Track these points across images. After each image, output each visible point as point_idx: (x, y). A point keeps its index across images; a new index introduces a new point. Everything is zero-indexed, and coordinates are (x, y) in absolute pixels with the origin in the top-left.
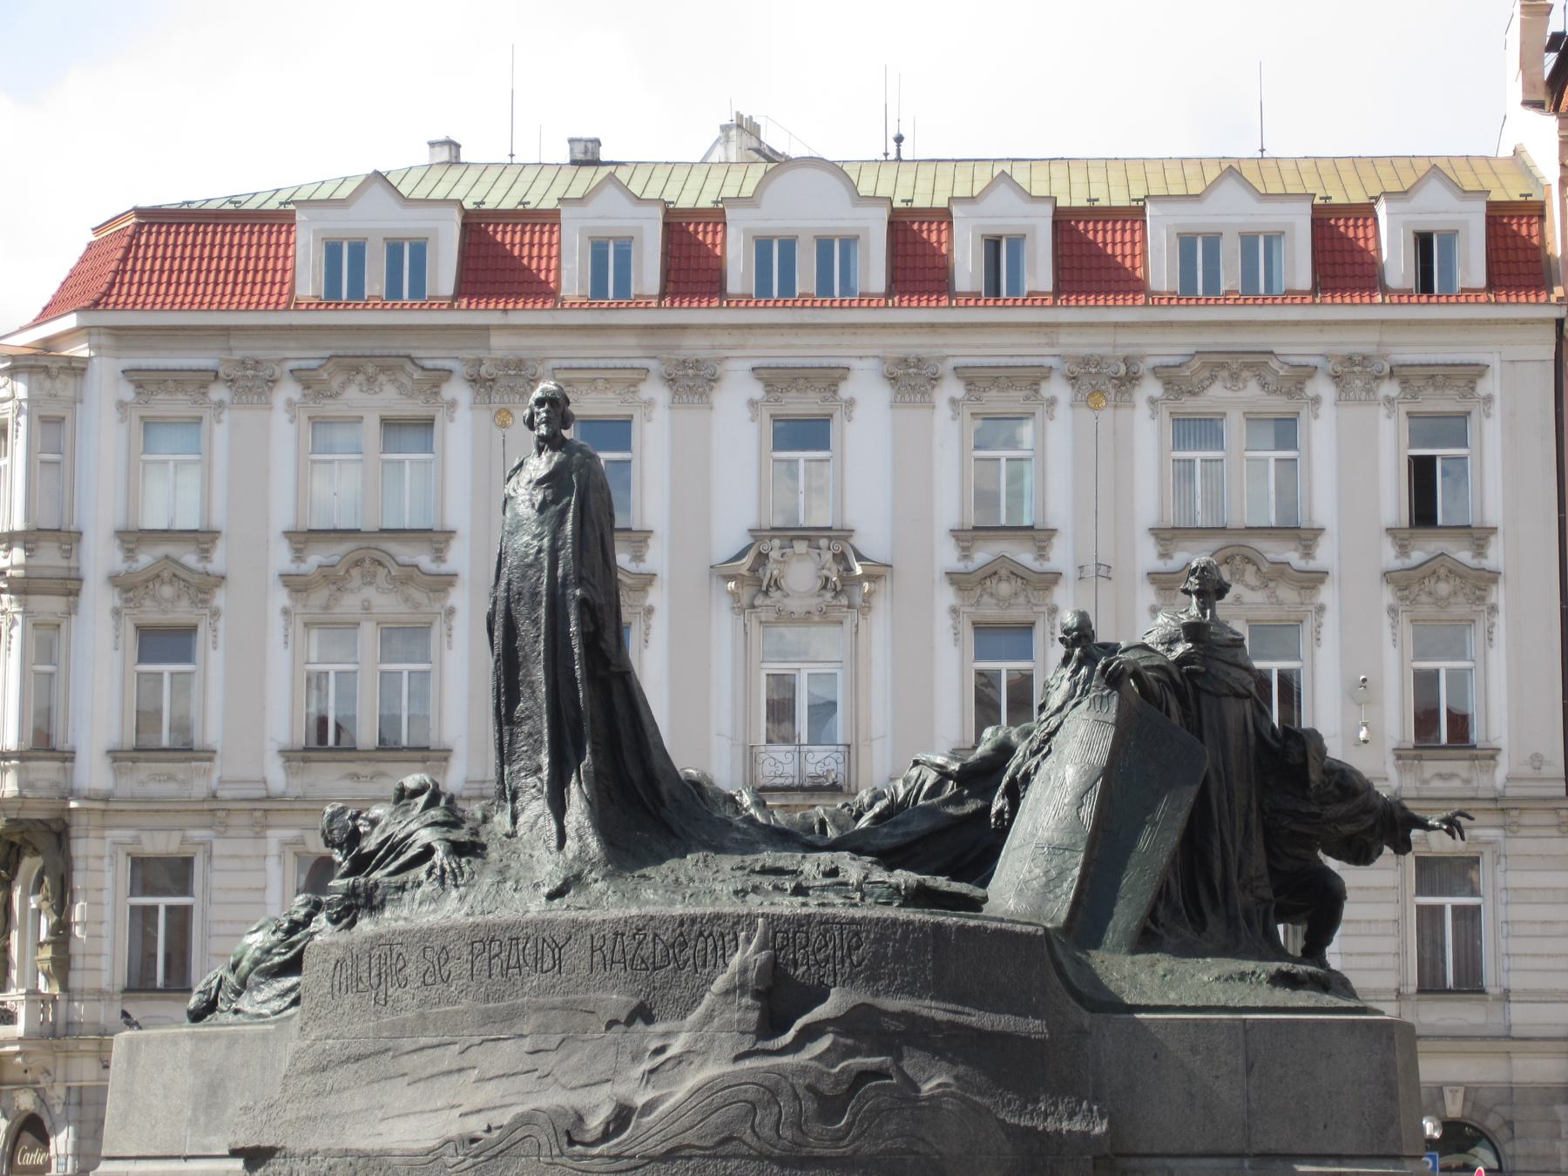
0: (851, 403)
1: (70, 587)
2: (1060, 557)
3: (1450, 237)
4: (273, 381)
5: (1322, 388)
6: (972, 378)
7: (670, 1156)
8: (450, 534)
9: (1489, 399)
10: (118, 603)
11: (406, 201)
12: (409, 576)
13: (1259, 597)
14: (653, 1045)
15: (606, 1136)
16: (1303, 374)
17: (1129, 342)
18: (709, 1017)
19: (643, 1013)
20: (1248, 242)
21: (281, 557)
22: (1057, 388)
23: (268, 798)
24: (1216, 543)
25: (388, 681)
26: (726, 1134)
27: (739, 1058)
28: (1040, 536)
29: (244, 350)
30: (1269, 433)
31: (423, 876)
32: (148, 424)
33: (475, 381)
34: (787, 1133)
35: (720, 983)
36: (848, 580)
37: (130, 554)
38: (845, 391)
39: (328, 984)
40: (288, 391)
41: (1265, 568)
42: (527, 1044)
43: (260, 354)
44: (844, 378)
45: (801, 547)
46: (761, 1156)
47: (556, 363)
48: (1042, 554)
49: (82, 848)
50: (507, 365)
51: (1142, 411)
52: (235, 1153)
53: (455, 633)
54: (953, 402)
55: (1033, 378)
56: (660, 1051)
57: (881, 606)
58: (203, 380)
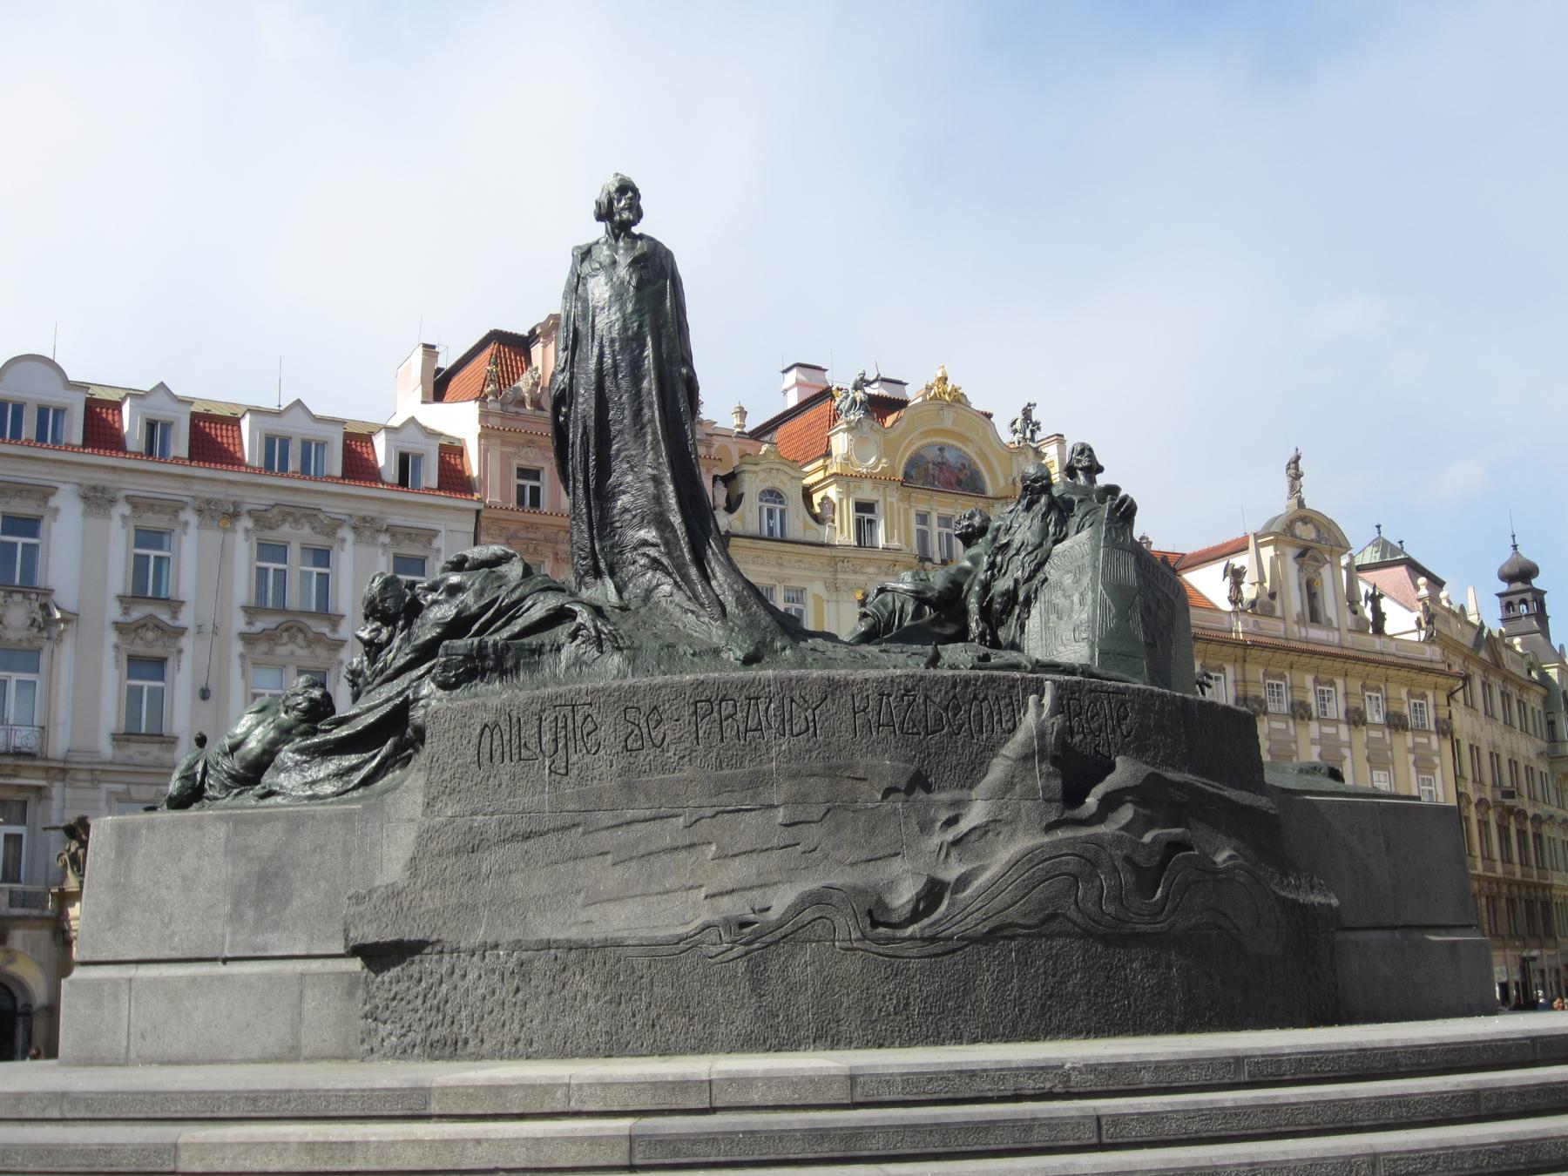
0: (56, 510)
2: (186, 618)
3: (419, 458)
5: (346, 533)
6: (135, 503)
7: (992, 936)
9: (438, 550)
13: (305, 652)
14: (944, 815)
15: (915, 916)
16: (337, 524)
17: (236, 493)
18: (1008, 785)
19: (919, 782)
20: (306, 445)
22: (189, 516)
24: (280, 619)
26: (1050, 910)
27: (1050, 828)
28: (175, 605)
30: (310, 556)
31: (563, 639)
34: (1109, 908)
35: (1013, 747)
36: (49, 620)
38: (53, 502)
39: (472, 751)
41: (310, 635)
42: (781, 815)
44: (53, 494)
45: (18, 597)
46: (1086, 934)
48: (175, 615)
51: (240, 535)
52: (357, 951)
54: (123, 517)
55: (175, 508)
56: (952, 822)
57: (69, 640)
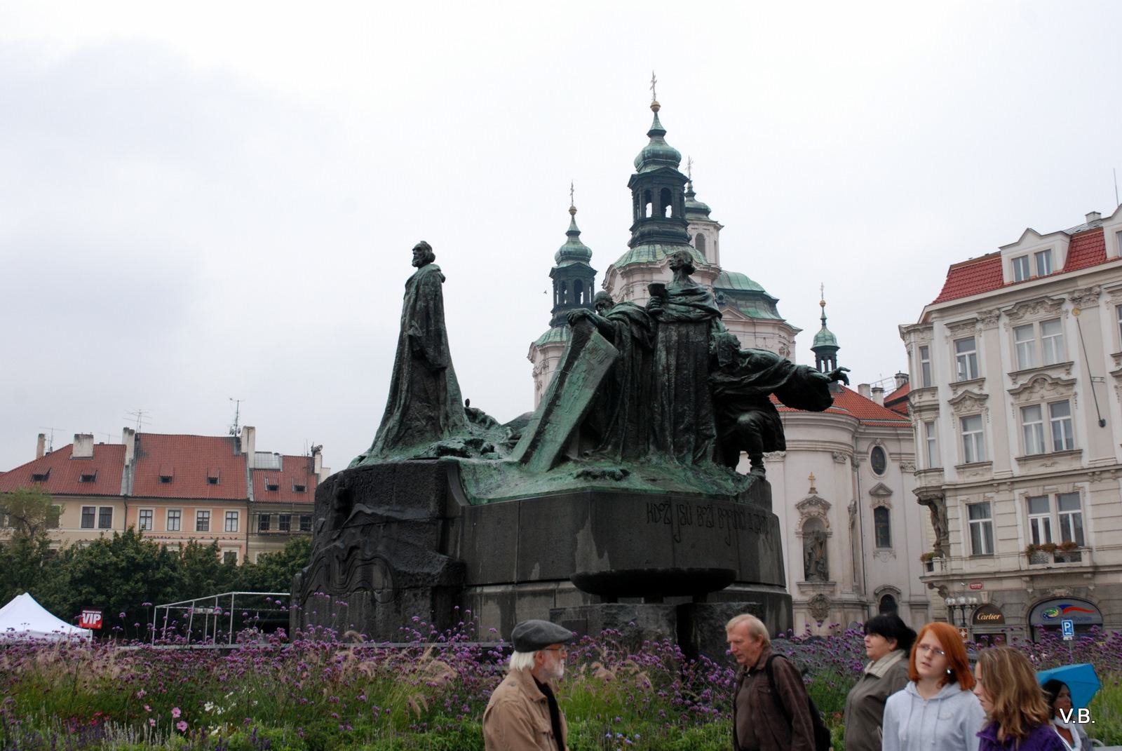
1: (935, 408)
4: (998, 317)
8: (1071, 364)
10: (953, 411)
11: (1041, 236)
12: (1056, 383)
21: (1009, 384)
23: (1013, 478)
25: (1055, 426)
29: (986, 308)
32: (957, 342)
33: (1073, 300)
37: (955, 391)
40: (1005, 320)
43: (990, 308)
47: (1106, 286)
49: (949, 502)
50: (1086, 290)
53: (1078, 402)
58: (974, 322)
